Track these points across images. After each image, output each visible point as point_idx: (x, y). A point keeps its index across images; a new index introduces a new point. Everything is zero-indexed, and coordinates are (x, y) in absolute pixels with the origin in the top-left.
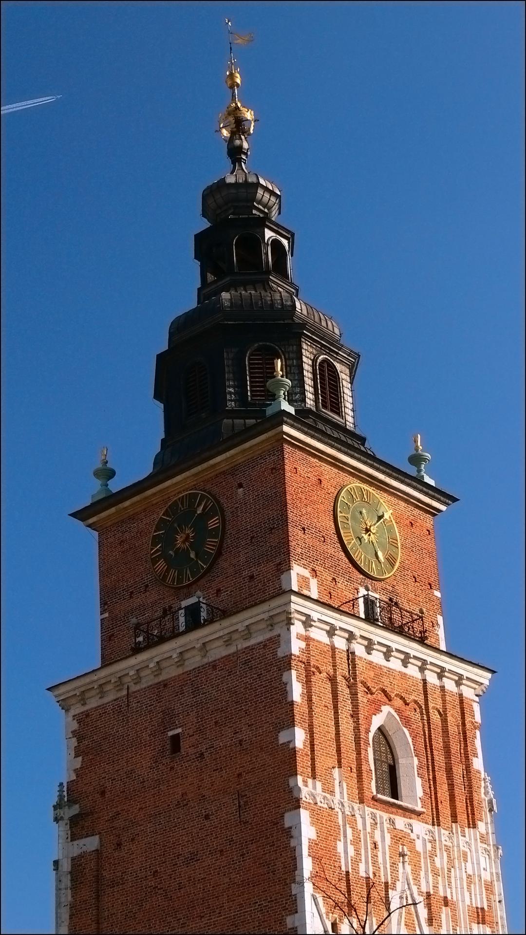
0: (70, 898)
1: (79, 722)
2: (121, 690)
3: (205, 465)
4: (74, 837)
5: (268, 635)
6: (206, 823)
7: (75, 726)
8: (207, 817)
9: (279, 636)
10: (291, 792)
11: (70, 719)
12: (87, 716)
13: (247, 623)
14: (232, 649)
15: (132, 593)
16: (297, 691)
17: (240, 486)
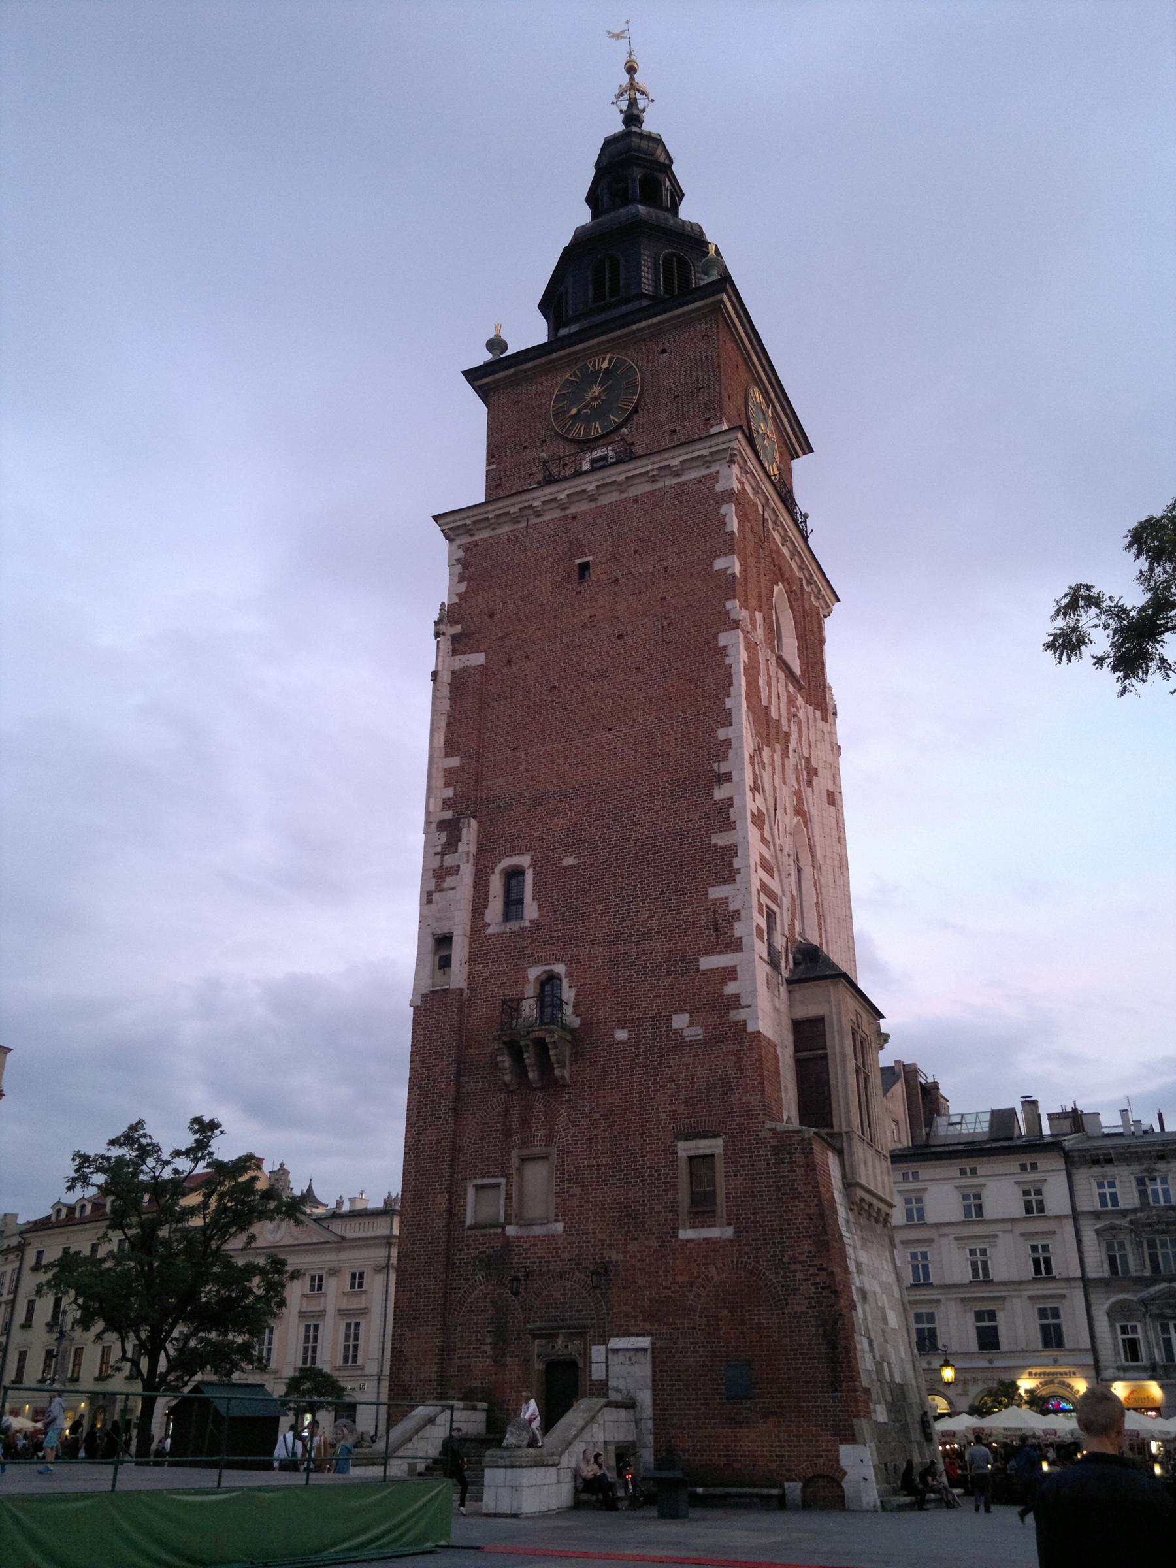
0: (448, 708)
1: (466, 551)
2: (519, 522)
3: (626, 330)
4: (455, 652)
6: (620, 643)
7: (460, 554)
8: (620, 637)
9: (718, 472)
10: (727, 613)
11: (454, 548)
12: (476, 545)
13: (682, 458)
15: (525, 447)
16: (734, 525)
17: (664, 351)
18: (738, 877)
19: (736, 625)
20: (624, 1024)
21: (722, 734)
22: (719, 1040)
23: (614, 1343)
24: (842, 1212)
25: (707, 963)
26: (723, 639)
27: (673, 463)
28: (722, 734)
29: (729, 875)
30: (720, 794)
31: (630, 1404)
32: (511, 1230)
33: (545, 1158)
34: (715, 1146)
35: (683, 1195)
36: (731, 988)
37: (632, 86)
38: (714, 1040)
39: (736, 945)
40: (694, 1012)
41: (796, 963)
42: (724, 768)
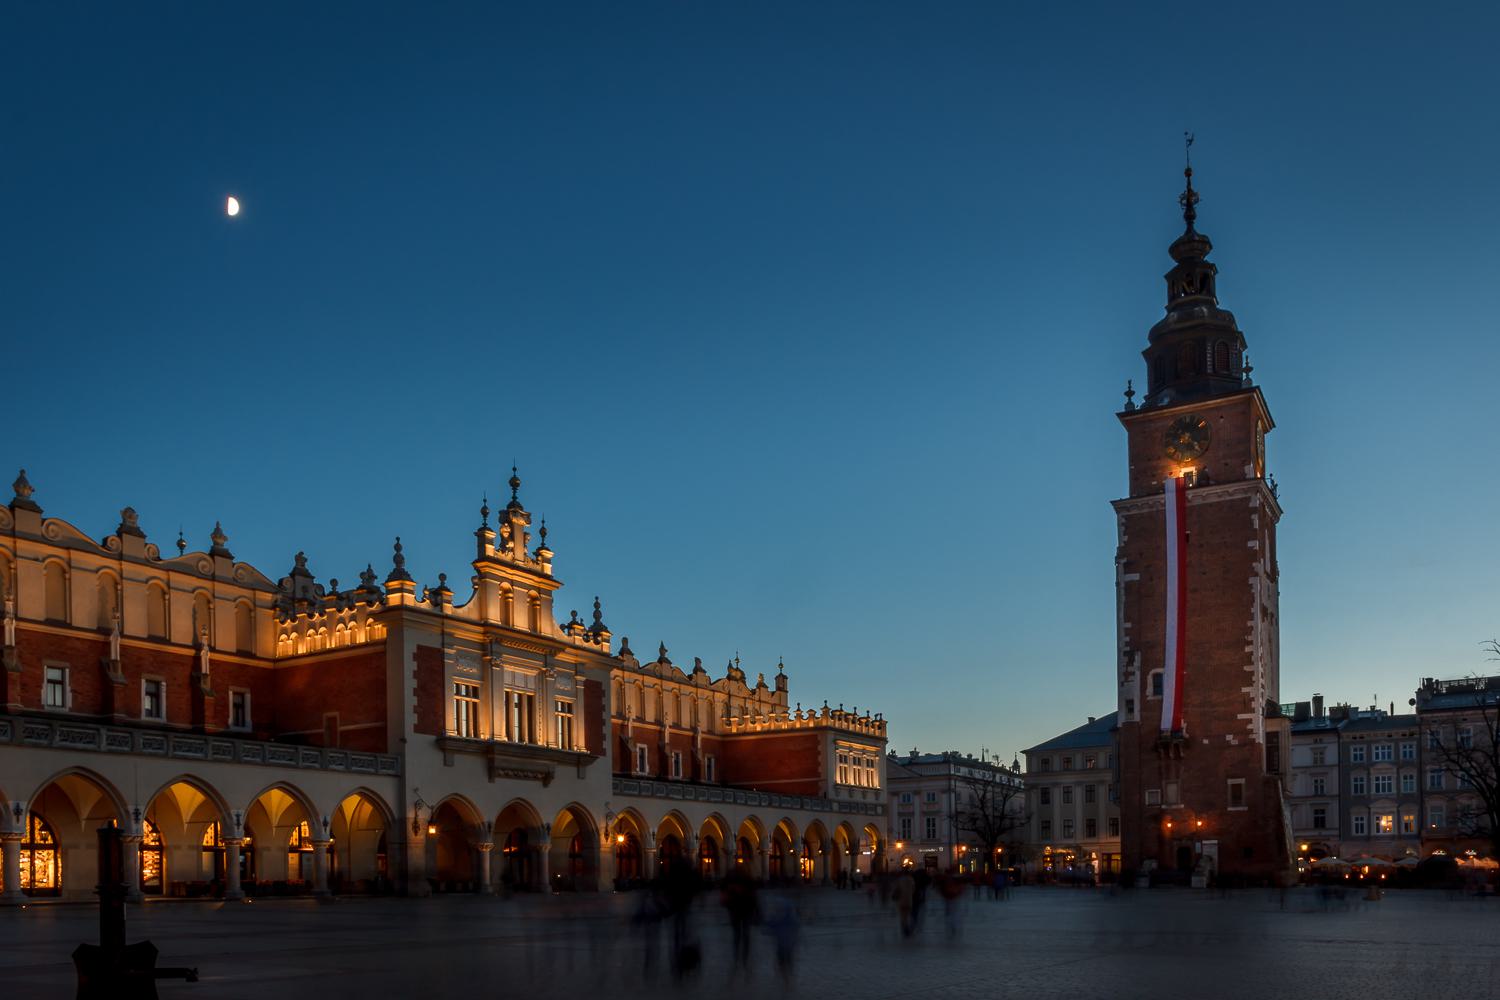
5: (1244, 496)
8: (1204, 574)
10: (1253, 568)
14: (1223, 499)
17: (1222, 417)
18: (1255, 685)
19: (1256, 575)
20: (1207, 737)
21: (1249, 624)
22: (1245, 745)
23: (1204, 842)
24: (1282, 800)
25: (1240, 716)
26: (1251, 580)
27: (1230, 490)
28: (1249, 624)
29: (1250, 684)
30: (1247, 649)
31: (1211, 859)
32: (1163, 807)
33: (1177, 783)
34: (1242, 781)
35: (1229, 797)
36: (1250, 727)
37: (1189, 190)
38: (1242, 745)
39: (1252, 711)
40: (1235, 735)
41: (1268, 709)
42: (1250, 638)
